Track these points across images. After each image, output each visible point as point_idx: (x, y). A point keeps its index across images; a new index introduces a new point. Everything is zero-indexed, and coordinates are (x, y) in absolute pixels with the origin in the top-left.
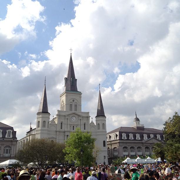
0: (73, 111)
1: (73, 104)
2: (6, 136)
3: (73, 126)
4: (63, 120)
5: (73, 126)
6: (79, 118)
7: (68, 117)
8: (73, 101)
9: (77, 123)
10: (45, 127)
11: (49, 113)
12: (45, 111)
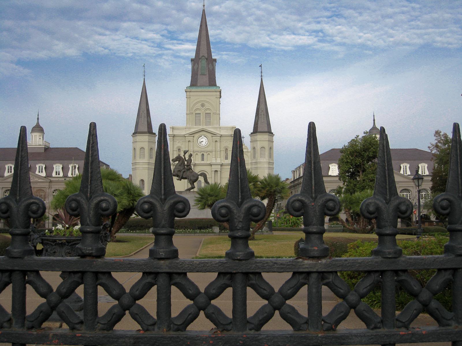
2: (70, 175)
3: (203, 155)
5: (203, 155)
6: (213, 138)
7: (192, 138)
8: (203, 105)
9: (209, 149)
10: (144, 157)
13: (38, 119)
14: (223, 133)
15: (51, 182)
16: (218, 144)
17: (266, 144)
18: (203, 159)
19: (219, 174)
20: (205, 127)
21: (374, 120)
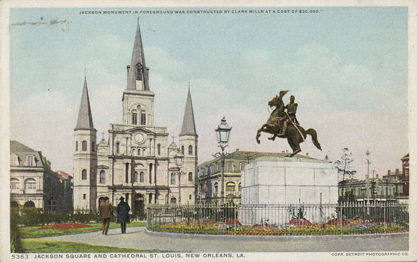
1: (138, 113)
4: (119, 137)
8: (139, 106)
16: (153, 141)
17: (193, 143)
18: (139, 154)
19: (153, 167)
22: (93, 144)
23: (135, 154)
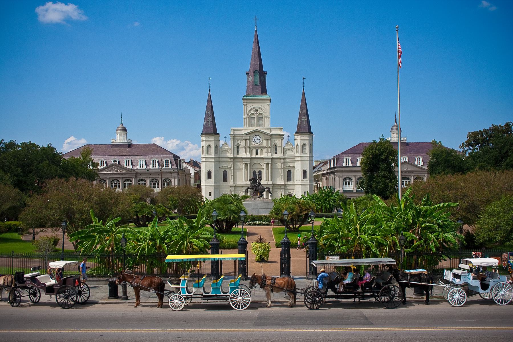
0: (256, 128)
1: (256, 116)
3: (257, 151)
5: (257, 151)
8: (256, 111)
11: (219, 134)
12: (211, 130)
13: (122, 121)
14: (272, 133)
15: (137, 173)
18: (257, 154)
20: (258, 128)
21: (396, 119)
22: (216, 147)
23: (254, 156)
